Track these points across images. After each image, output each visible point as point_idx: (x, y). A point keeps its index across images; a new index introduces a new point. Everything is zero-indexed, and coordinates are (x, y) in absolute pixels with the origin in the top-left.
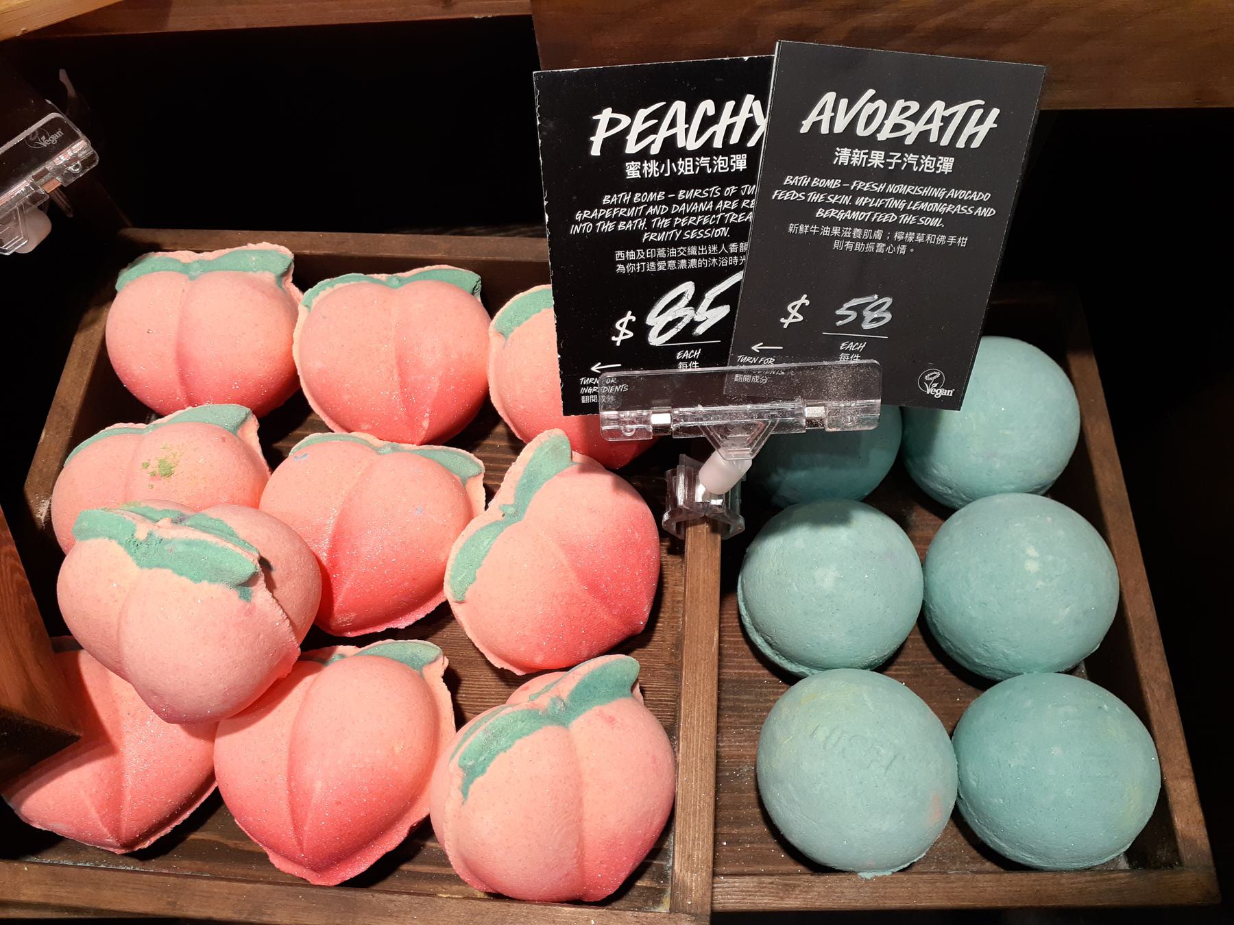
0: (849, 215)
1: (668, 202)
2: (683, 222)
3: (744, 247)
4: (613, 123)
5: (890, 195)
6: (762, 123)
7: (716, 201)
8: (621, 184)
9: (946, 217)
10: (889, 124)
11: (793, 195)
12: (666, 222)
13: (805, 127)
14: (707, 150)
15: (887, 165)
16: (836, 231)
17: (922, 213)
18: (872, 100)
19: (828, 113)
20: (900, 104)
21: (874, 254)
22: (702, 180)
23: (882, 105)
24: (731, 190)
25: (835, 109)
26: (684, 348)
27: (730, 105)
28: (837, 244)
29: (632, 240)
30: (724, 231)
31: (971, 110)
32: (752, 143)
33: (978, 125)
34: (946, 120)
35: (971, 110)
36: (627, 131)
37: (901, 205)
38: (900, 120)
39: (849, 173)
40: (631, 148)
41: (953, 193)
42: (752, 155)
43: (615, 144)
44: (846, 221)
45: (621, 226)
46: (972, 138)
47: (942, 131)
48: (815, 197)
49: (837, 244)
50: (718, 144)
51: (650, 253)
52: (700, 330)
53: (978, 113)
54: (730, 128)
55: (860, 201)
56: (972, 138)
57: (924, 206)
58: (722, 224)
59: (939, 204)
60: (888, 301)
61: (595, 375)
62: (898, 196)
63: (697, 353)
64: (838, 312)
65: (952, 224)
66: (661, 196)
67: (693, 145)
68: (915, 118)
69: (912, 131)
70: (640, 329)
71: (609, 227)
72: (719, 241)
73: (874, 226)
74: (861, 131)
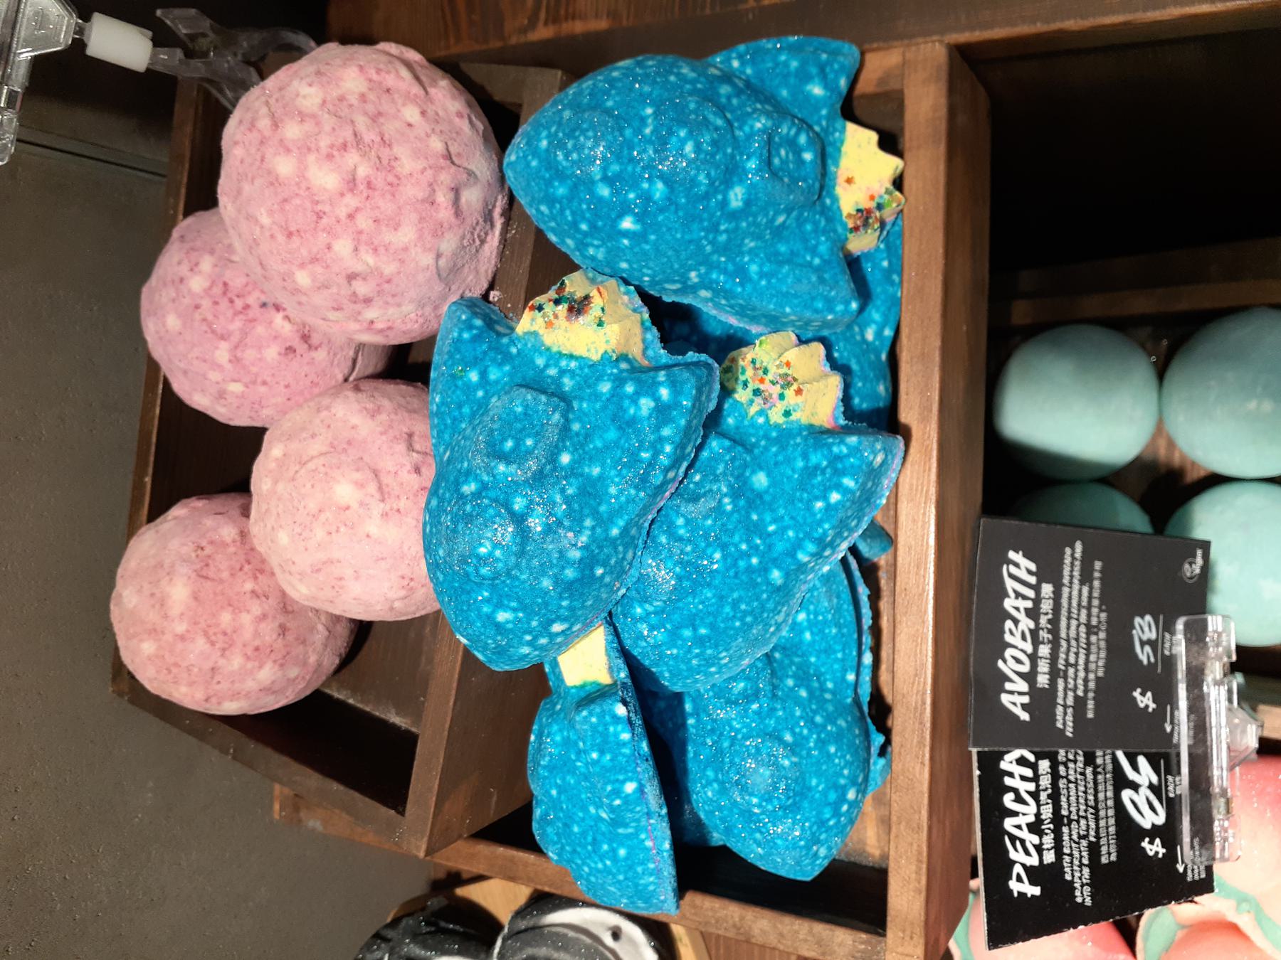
0: (1081, 667)
1: (1070, 821)
2: (1083, 807)
3: (1099, 753)
4: (1019, 879)
5: (1068, 635)
6: (1017, 753)
7: (1070, 782)
8: (1057, 866)
9: (1082, 583)
10: (1021, 644)
11: (1069, 718)
12: (1083, 822)
13: (1025, 716)
14: (1035, 795)
15: (1049, 642)
16: (1092, 676)
17: (1079, 605)
18: (1005, 661)
19: (1014, 700)
20: (1008, 638)
21: (1107, 641)
22: (1055, 797)
23: (1009, 653)
24: (1062, 769)
25: (1012, 693)
26: (1167, 791)
27: (1008, 781)
28: (1100, 674)
29: (1094, 849)
30: (1089, 770)
31: (1011, 576)
32: (1031, 758)
33: (1021, 565)
34: (1018, 595)
35: (1011, 576)
36: (1024, 865)
37: (1074, 623)
38: (1018, 635)
39: (1054, 673)
40: (1033, 861)
41: (1066, 580)
42: (1039, 757)
43: (1034, 874)
44: (1086, 666)
45: (1085, 861)
46: (1029, 572)
47: (1025, 598)
48: (1070, 701)
49: (1100, 674)
50: (1031, 787)
51: (1103, 833)
52: (1155, 780)
53: (1013, 569)
54: (1023, 778)
55: (1072, 660)
56: (1029, 572)
57: (1074, 603)
58: (1083, 774)
59: (1074, 591)
60: (1137, 620)
61: (1185, 869)
62: (1068, 628)
63: (1170, 778)
64: (1145, 662)
65: (1086, 578)
66: (1065, 830)
67: (1032, 808)
68: (1016, 622)
69: (1026, 624)
70: (1155, 832)
71: (1086, 871)
72: (1095, 773)
73: (1089, 644)
74: (1025, 668)
